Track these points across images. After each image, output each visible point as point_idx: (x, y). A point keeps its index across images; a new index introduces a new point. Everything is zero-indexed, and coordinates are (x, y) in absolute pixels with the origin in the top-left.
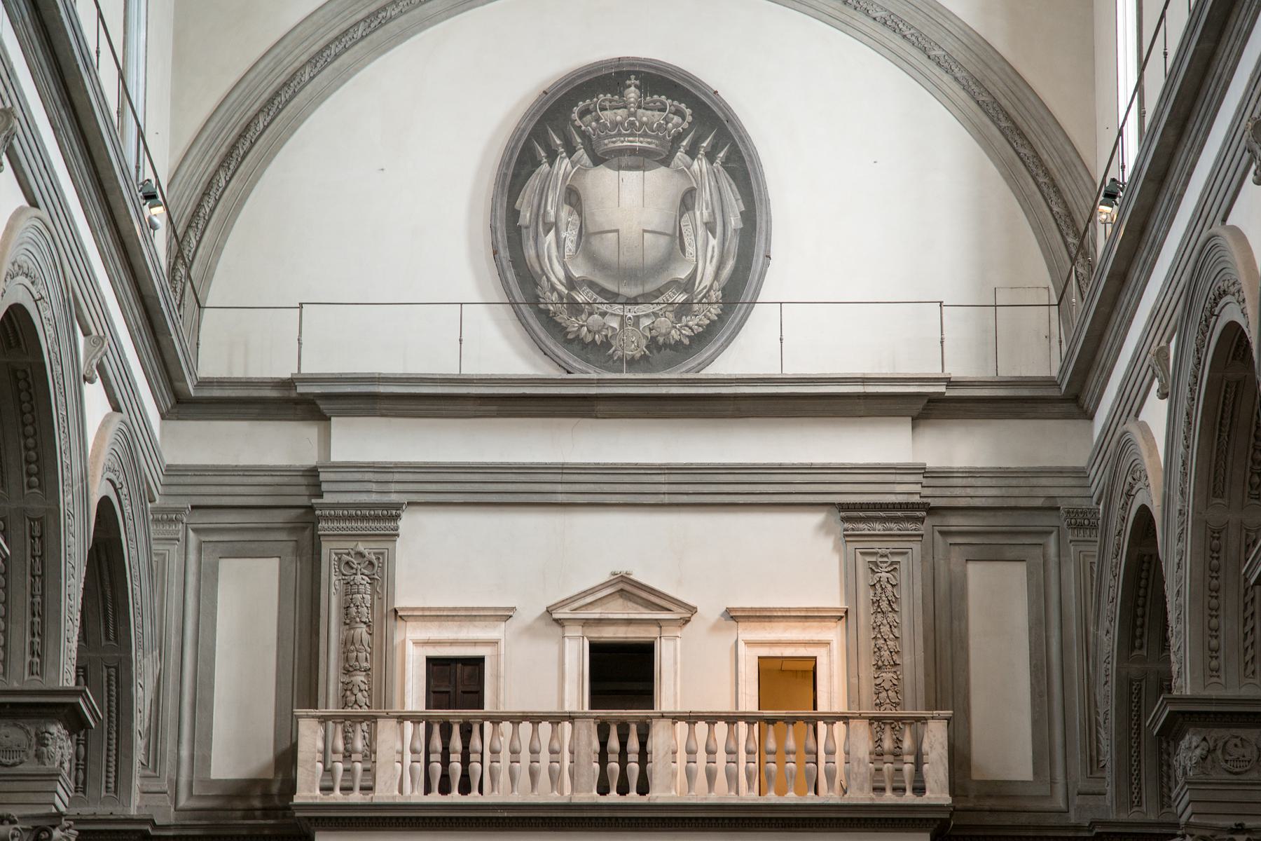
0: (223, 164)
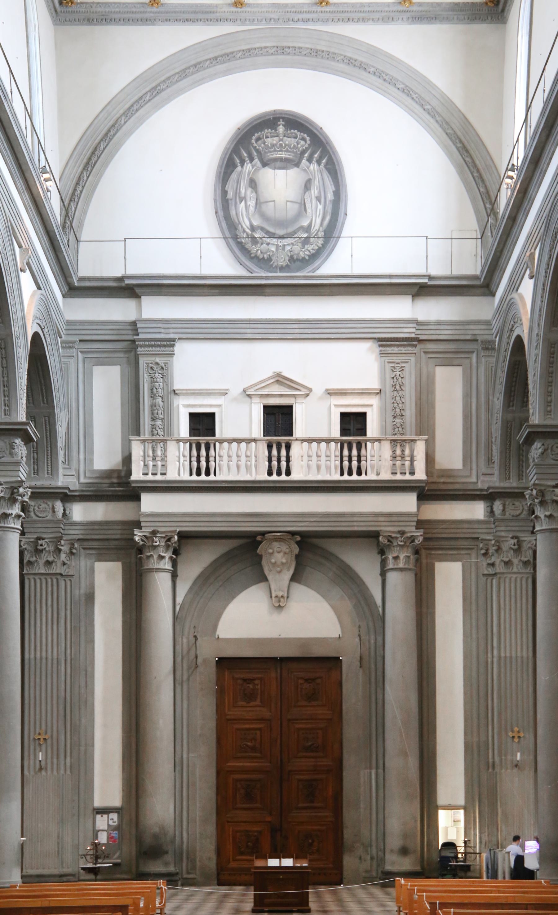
0: (85, 168)
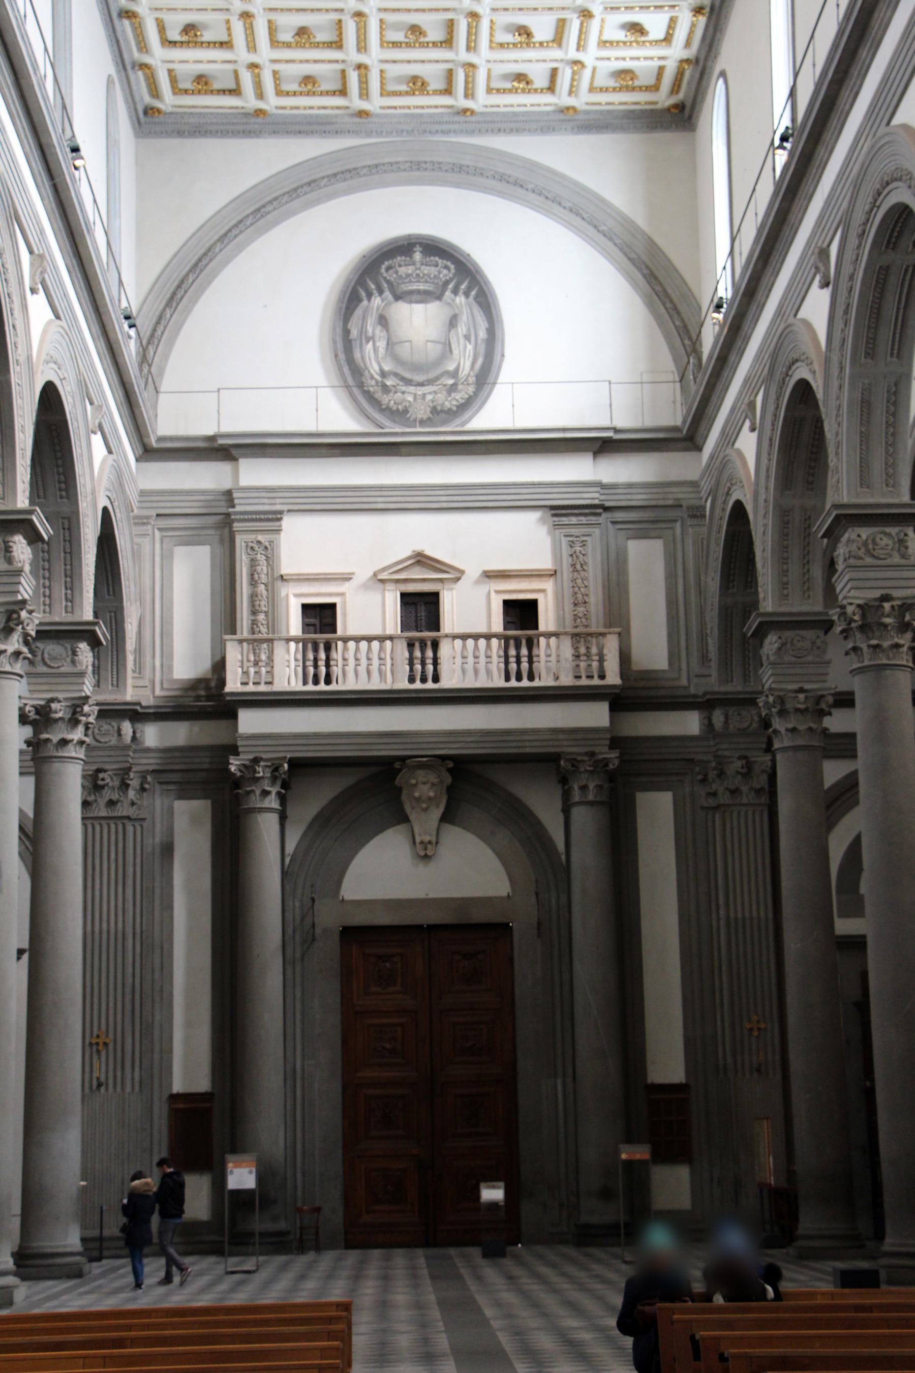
0: (168, 304)
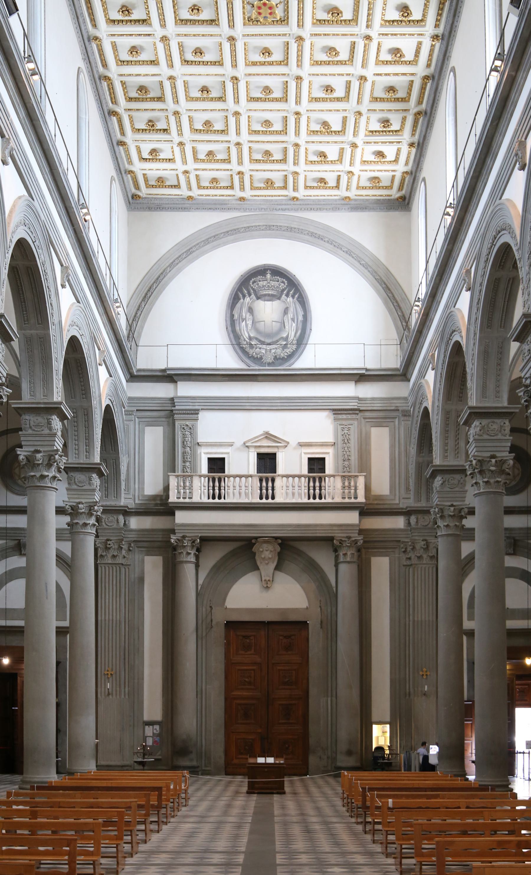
0: (143, 300)
